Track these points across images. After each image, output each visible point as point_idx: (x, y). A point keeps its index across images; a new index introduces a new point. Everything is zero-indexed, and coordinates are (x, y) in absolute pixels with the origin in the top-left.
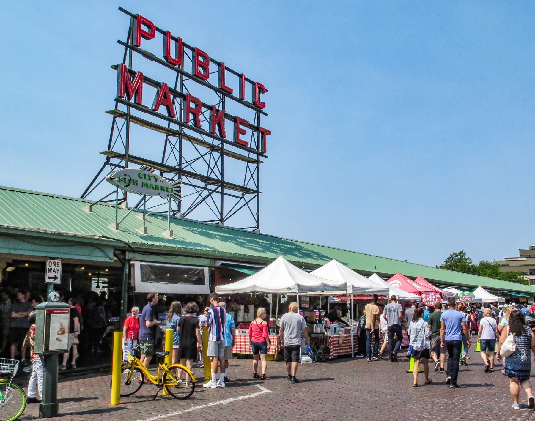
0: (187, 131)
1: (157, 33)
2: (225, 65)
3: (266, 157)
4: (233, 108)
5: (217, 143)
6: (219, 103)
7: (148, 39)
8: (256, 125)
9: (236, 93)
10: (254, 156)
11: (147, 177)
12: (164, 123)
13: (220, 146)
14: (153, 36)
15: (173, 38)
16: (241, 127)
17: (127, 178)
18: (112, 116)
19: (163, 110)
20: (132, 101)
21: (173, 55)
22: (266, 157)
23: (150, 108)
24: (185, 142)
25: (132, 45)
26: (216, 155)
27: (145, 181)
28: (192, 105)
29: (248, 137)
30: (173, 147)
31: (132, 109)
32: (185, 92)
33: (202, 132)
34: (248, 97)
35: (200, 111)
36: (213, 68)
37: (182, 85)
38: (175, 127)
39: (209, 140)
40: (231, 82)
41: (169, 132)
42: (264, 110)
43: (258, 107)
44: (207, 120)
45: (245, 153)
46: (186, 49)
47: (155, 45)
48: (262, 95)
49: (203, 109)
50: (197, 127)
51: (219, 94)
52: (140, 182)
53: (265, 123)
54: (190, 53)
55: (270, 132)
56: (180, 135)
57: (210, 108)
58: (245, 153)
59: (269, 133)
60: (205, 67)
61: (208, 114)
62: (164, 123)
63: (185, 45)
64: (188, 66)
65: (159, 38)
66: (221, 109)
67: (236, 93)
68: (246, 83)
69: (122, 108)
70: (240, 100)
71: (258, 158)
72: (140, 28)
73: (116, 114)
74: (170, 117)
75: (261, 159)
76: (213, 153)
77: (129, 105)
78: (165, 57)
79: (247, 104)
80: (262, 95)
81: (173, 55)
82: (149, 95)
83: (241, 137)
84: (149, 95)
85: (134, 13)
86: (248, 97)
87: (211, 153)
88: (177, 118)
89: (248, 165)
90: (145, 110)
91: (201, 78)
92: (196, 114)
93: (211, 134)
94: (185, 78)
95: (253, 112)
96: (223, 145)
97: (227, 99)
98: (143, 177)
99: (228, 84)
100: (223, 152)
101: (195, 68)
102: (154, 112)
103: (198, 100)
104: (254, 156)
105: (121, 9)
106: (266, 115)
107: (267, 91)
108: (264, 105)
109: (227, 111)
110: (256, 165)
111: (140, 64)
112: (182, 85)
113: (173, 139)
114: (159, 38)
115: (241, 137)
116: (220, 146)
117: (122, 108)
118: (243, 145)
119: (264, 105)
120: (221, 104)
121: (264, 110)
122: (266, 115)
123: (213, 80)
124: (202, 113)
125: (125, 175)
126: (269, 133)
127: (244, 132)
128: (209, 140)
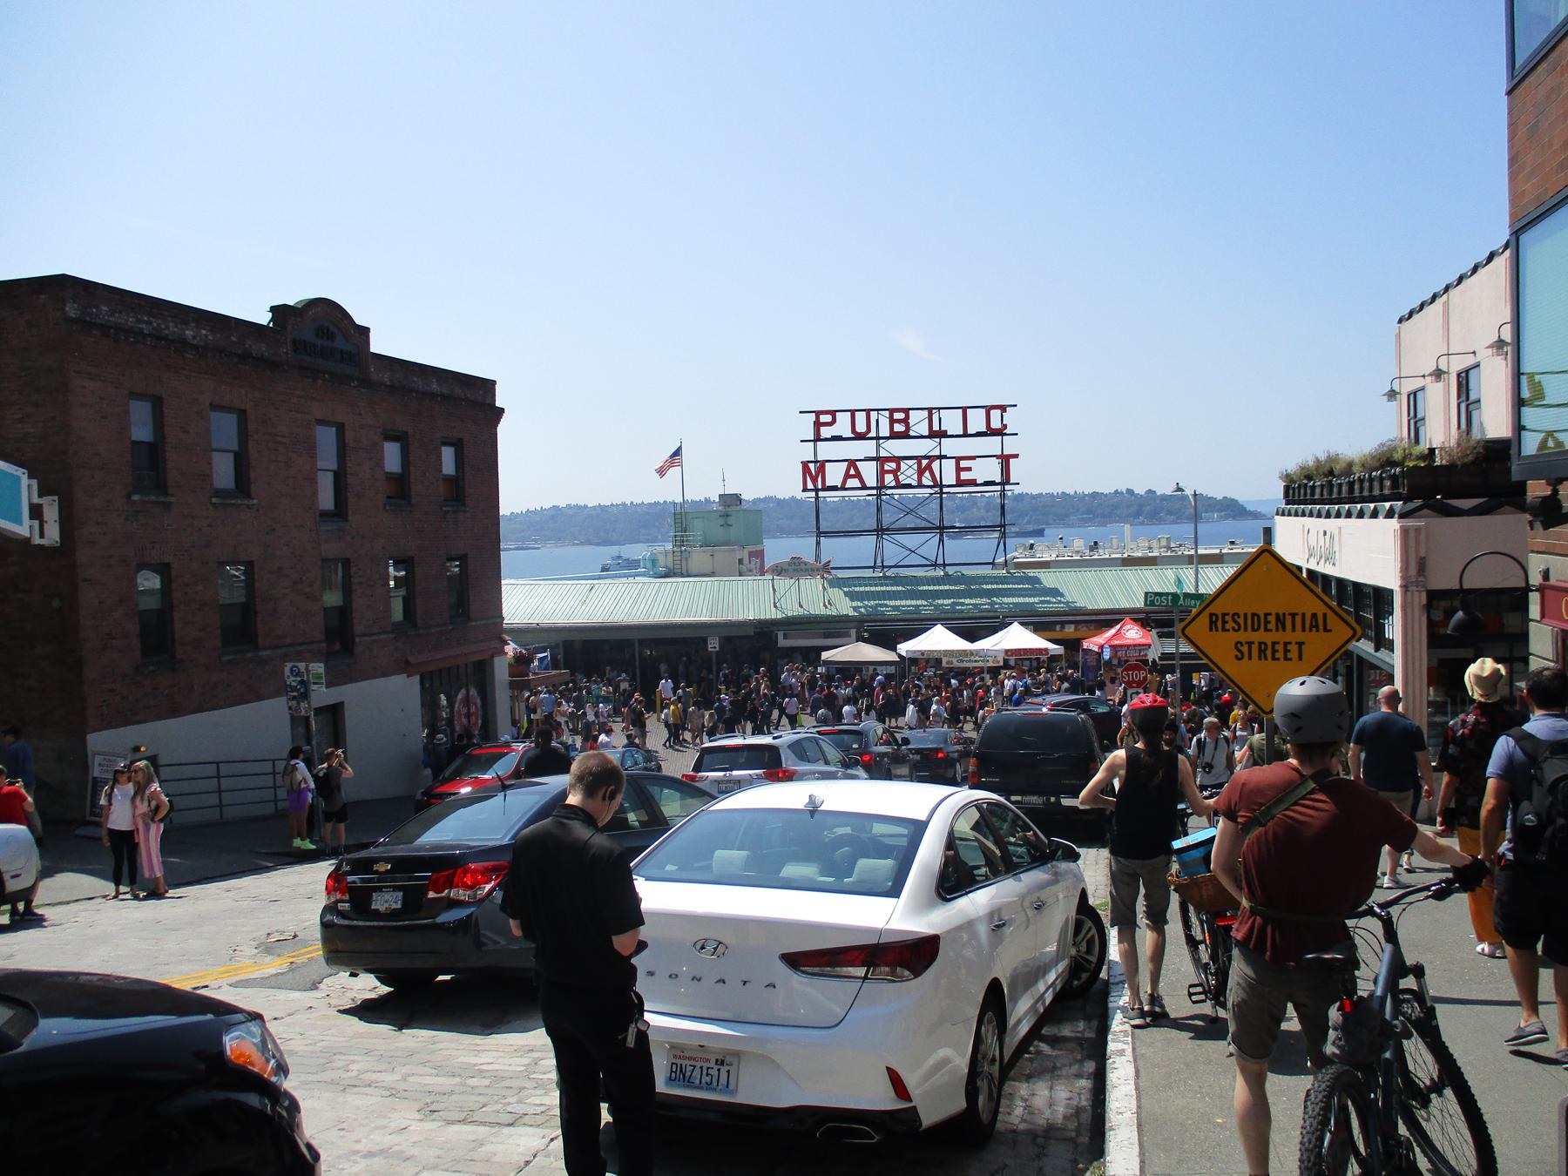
32: (883, 454)
47: (843, 427)
49: (910, 462)
60: (905, 421)
65: (843, 421)
70: (965, 435)
74: (864, 487)
79: (979, 434)
81: (861, 428)
83: (964, 476)
92: (895, 472)
102: (843, 488)
111: (826, 450)
118: (973, 483)
126: (1016, 456)
127: (969, 469)
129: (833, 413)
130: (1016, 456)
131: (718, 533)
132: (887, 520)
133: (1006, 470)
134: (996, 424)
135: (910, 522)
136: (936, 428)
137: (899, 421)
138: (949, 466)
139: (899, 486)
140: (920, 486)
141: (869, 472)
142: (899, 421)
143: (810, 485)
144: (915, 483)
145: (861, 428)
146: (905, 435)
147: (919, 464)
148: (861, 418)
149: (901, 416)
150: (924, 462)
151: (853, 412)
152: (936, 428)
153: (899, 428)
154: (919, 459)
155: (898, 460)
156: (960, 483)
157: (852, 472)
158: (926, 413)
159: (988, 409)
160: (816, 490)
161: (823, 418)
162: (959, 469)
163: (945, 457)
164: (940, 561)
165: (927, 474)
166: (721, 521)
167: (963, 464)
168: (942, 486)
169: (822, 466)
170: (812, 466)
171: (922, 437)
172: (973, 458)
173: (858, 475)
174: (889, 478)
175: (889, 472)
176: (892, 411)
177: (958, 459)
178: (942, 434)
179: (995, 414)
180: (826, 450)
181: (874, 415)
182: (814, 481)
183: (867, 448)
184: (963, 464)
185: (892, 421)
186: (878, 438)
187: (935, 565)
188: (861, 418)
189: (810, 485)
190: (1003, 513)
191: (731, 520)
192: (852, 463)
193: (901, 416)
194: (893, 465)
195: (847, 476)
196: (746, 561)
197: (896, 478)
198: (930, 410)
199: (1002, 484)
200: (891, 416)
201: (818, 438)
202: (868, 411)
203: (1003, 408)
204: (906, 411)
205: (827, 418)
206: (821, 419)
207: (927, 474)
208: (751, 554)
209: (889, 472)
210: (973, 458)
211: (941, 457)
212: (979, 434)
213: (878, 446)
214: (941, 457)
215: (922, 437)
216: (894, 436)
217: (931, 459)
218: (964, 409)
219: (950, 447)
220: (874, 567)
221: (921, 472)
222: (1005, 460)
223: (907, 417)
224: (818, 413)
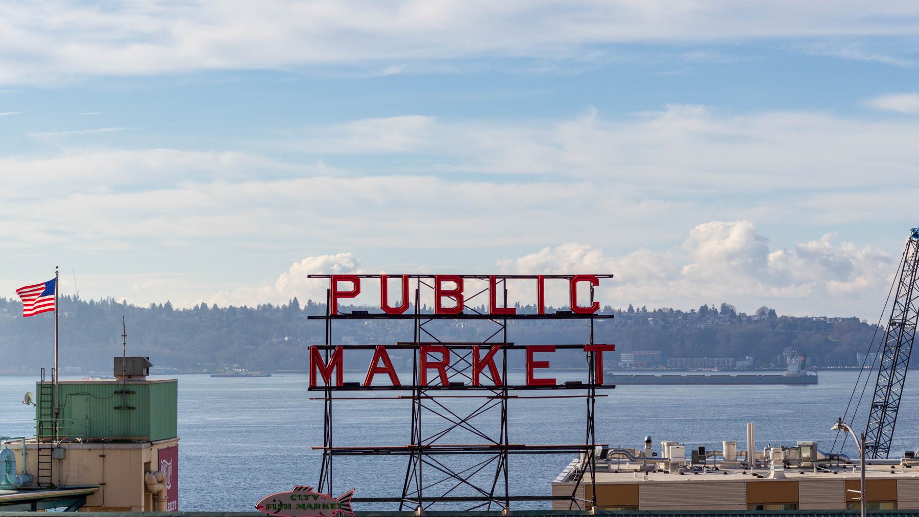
11: (303, 498)
17: (277, 503)
20: (334, 383)
23: (362, 383)
27: (301, 503)
32: (424, 338)
33: (460, 386)
49: (462, 352)
52: (294, 504)
53: (603, 333)
60: (457, 294)
61: (470, 359)
63: (419, 277)
70: (542, 315)
74: (397, 386)
75: (598, 391)
83: (539, 374)
90: (355, 386)
92: (441, 367)
94: (422, 321)
96: (506, 393)
98: (297, 498)
102: (368, 387)
105: (309, 276)
111: (343, 332)
118: (550, 384)
125: (274, 501)
126: (611, 348)
127: (545, 365)
129: (355, 279)
130: (611, 348)
131: (114, 422)
132: (427, 436)
133: (596, 365)
134: (583, 301)
135: (461, 437)
136: (499, 304)
137: (448, 293)
138: (517, 357)
140: (477, 386)
141: (402, 360)
142: (448, 293)
143: (320, 381)
144: (468, 382)
145: (394, 300)
146: (457, 314)
147: (476, 355)
148: (395, 287)
149: (450, 286)
150: (483, 353)
151: (384, 279)
152: (499, 304)
153: (448, 303)
154: (475, 348)
155: (445, 348)
156: (533, 384)
157: (381, 364)
158: (486, 283)
159: (574, 280)
160: (328, 389)
161: (346, 286)
162: (531, 365)
163: (511, 346)
164: (500, 491)
165: (486, 369)
166: (117, 400)
167: (538, 357)
168: (506, 388)
169: (338, 353)
170: (322, 352)
171: (480, 317)
172: (551, 349)
173: (390, 370)
175: (432, 365)
176: (439, 279)
177: (531, 350)
178: (507, 314)
179: (583, 287)
180: (343, 332)
181: (413, 283)
182: (327, 376)
183: (402, 330)
184: (538, 357)
185: (439, 293)
186: (417, 316)
187: (490, 498)
188: (395, 287)
189: (320, 381)
190: (591, 429)
191: (132, 400)
192: (381, 351)
193: (450, 286)
194: (439, 356)
195: (375, 370)
196: (154, 467)
198: (493, 279)
199: (591, 386)
200: (438, 285)
201: (333, 314)
202: (406, 279)
203: (594, 280)
204: (459, 279)
205: (348, 286)
207: (486, 369)
208: (162, 454)
209: (432, 365)
210: (551, 349)
211: (507, 346)
212: (561, 315)
213: (417, 329)
214: (507, 346)
215: (480, 317)
216: (442, 314)
217: (492, 348)
218: (541, 279)
219: (517, 331)
220: (401, 500)
221: (478, 367)
222: (596, 353)
223: (461, 288)
224: (335, 279)
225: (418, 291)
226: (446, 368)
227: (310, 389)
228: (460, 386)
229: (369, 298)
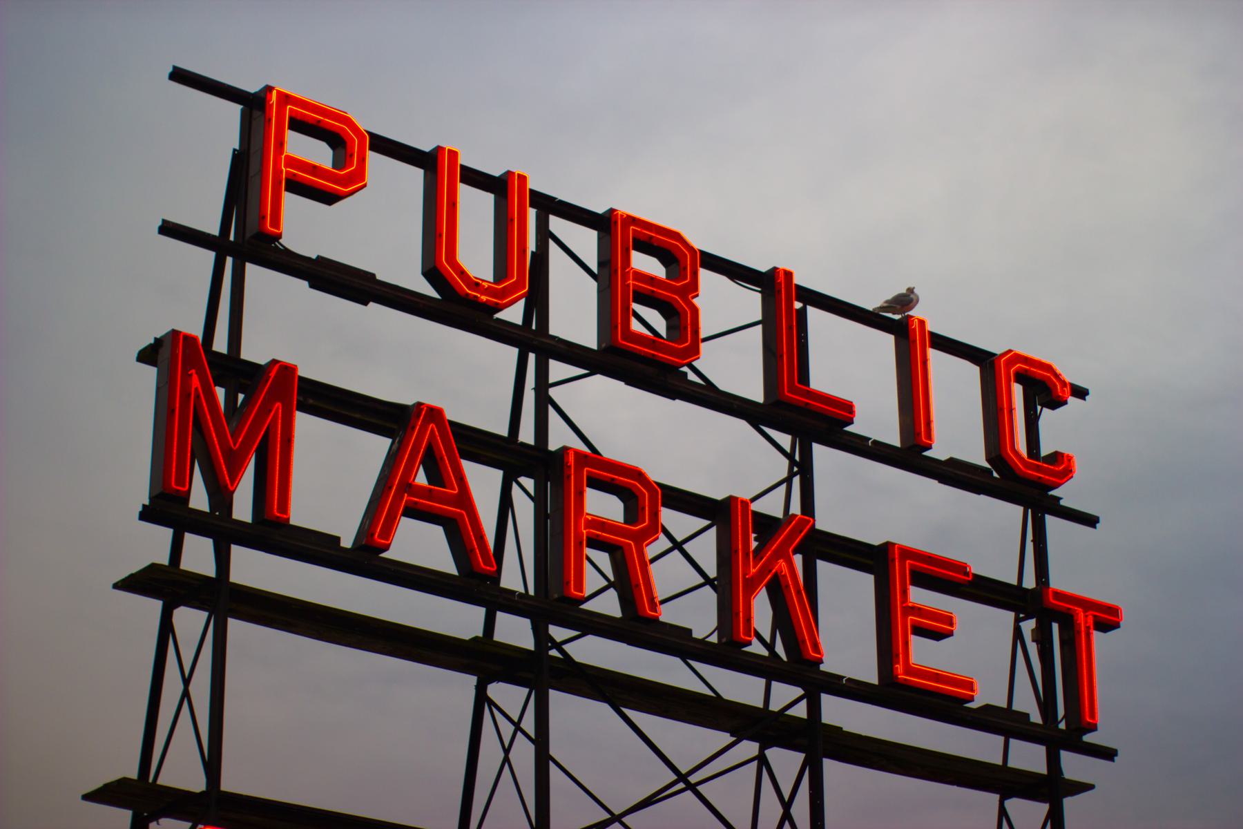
0: (593, 651)
1: (376, 163)
2: (797, 280)
3: (1108, 754)
4: (858, 498)
5: (784, 694)
6: (788, 481)
7: (329, 198)
8: (1030, 582)
9: (878, 418)
10: (1029, 757)
12: (459, 620)
13: (801, 711)
14: (356, 179)
15: (475, 178)
16: (919, 596)
18: (155, 606)
19: (420, 544)
20: (243, 508)
21: (476, 255)
22: (1108, 754)
23: (347, 542)
24: (566, 708)
25: (246, 240)
26: (787, 762)
28: (603, 506)
29: (979, 650)
30: (507, 729)
31: (239, 554)
32: (559, 436)
33: (677, 642)
34: (958, 430)
35: (656, 528)
36: (723, 305)
37: (544, 402)
38: (515, 631)
39: (743, 689)
40: (848, 364)
41: (481, 660)
42: (1067, 494)
43: (1026, 482)
44: (708, 581)
45: (981, 747)
46: (557, 224)
47: (378, 226)
48: (1047, 417)
49: (677, 522)
50: (640, 625)
51: (785, 440)
53: (1076, 566)
54: (585, 241)
55: (1114, 611)
56: (544, 673)
57: (719, 512)
58: (981, 747)
59: (1107, 618)
61: (706, 550)
62: (459, 620)
63: (548, 205)
64: (574, 312)
66: (796, 508)
67: (878, 418)
68: (939, 363)
69: (199, 556)
70: (911, 454)
71: (1053, 761)
72: (278, 157)
73: (163, 584)
74: (474, 580)
75: (1073, 765)
76: (773, 754)
77: (226, 534)
78: (432, 273)
79: (954, 474)
80: (1047, 417)
81: (476, 255)
82: (333, 474)
83: (923, 653)
84: (333, 474)
85: (252, 86)
86: (958, 430)
87: (762, 760)
88: (515, 575)
89: (1003, 813)
90: (316, 549)
91: (659, 368)
93: (728, 651)
94: (558, 370)
95: (1010, 514)
96: (815, 708)
97: (822, 454)
99: (825, 376)
100: (820, 744)
101: (611, 313)
102: (366, 558)
103: (638, 474)
104: (1029, 757)
105: (179, 75)
106: (1090, 521)
107: (1081, 393)
108: (1061, 466)
109: (827, 520)
110: (1044, 808)
111: (284, 324)
112: (544, 402)
113: (509, 696)
114: (394, 190)
115: (923, 653)
116: (801, 711)
117: (199, 556)
118: (944, 701)
119: (1061, 466)
120: (796, 481)
121: (1067, 494)
122: (1090, 521)
123: (737, 365)
124: (678, 546)
126: (1107, 618)
127: (938, 628)
128: (743, 689)
139: (640, 625)
148: (475, 211)
174: (596, 570)
188: (475, 211)
195: (390, 500)
197: (629, 580)
203: (1045, 389)
206: (278, 157)
209: (601, 536)
216: (619, 358)
225: (541, 259)
226: (651, 551)
227: (147, 515)
228: (677, 642)
229: (378, 226)
